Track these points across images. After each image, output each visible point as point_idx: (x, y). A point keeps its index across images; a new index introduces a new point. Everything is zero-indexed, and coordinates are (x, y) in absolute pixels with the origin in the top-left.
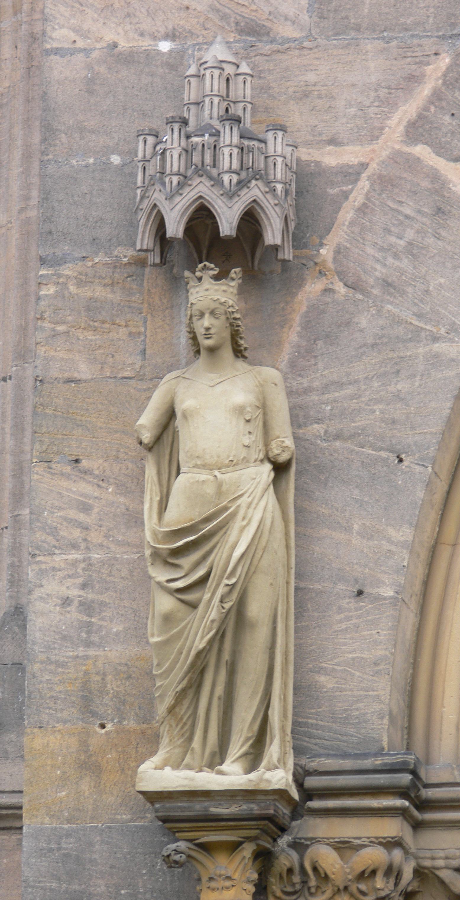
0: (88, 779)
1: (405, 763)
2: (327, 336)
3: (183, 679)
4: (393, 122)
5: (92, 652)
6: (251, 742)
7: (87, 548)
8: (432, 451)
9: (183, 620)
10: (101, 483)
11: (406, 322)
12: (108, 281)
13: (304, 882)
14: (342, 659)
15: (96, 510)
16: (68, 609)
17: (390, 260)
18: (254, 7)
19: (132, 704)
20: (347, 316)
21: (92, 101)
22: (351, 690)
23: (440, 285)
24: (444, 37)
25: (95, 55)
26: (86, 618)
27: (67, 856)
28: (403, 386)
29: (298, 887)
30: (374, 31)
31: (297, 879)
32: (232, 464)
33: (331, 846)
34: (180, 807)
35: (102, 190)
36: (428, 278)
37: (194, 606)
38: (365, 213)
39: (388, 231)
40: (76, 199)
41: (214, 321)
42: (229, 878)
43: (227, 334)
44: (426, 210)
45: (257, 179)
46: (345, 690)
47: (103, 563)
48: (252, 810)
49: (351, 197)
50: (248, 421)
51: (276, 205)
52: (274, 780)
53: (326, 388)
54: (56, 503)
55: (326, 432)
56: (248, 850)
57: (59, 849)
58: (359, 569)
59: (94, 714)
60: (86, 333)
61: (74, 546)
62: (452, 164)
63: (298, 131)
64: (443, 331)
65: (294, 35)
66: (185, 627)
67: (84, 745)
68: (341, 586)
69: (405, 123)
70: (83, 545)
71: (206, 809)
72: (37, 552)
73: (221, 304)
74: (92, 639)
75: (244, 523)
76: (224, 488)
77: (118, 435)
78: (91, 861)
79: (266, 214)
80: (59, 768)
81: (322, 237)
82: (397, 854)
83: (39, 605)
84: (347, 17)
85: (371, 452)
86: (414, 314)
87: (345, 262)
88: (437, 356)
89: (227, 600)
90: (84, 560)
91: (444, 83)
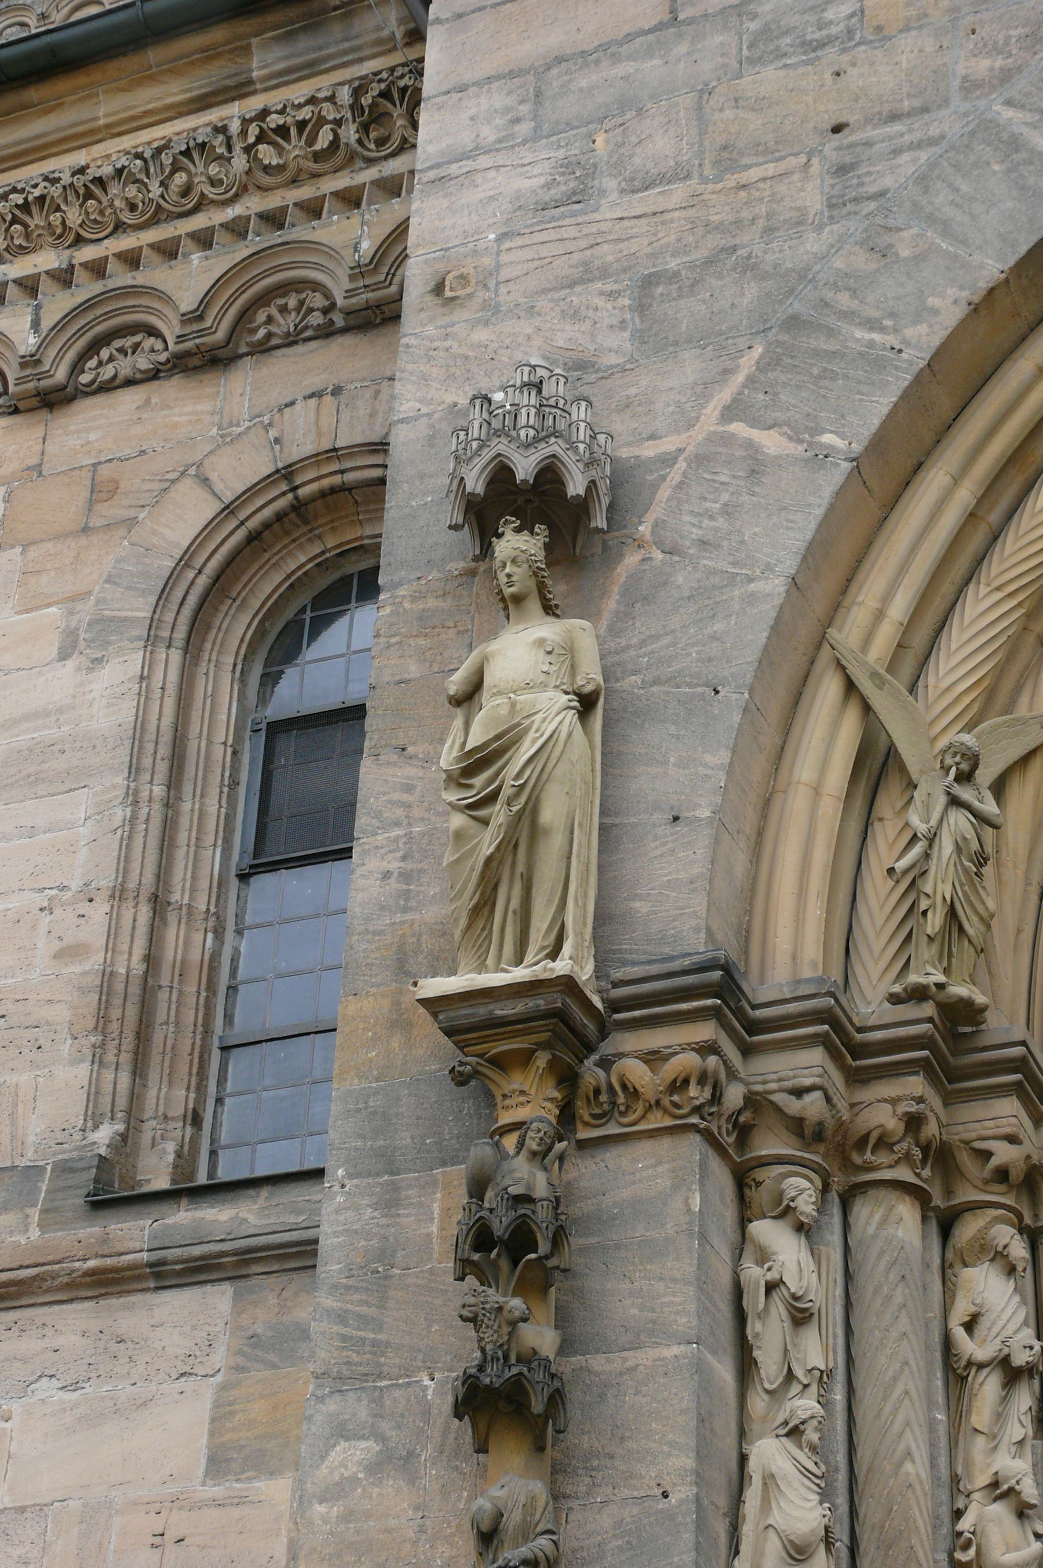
0: (399, 1036)
1: (715, 959)
2: (645, 598)
3: (474, 894)
4: (708, 411)
5: (409, 917)
6: (547, 951)
7: (409, 823)
8: (749, 678)
9: (473, 837)
10: (425, 764)
11: (722, 572)
12: (440, 592)
13: (614, 1104)
14: (658, 883)
15: (418, 789)
16: (388, 881)
17: (706, 522)
18: (581, 349)
19: (446, 959)
20: (664, 578)
21: (433, 452)
22: (666, 911)
23: (755, 534)
24: (758, 333)
25: (436, 416)
26: (404, 887)
27: (374, 1113)
28: (719, 627)
29: (606, 1107)
30: (691, 342)
31: (604, 1098)
32: (528, 686)
33: (640, 1059)
34: (464, 1015)
35: (439, 520)
36: (743, 530)
37: (485, 822)
38: (681, 489)
39: (704, 499)
40: (414, 532)
41: (516, 569)
42: (522, 1092)
43: (532, 583)
44: (740, 474)
45: (556, 437)
46: (660, 912)
47: (423, 834)
48: (538, 1006)
49: (669, 479)
50: (549, 653)
51: (578, 461)
52: (558, 968)
53: (643, 643)
54: (382, 789)
55: (643, 680)
56: (542, 1059)
57: (366, 1108)
58: (675, 797)
59: (408, 974)
60: (417, 640)
61: (397, 824)
62: (766, 432)
63: (620, 435)
64: (758, 572)
65: (617, 362)
66: (478, 844)
67: (397, 1003)
68: (657, 816)
69: (720, 408)
70: (405, 822)
71: (491, 1013)
72: (361, 836)
73: (522, 551)
74: (409, 905)
75: (537, 735)
76: (518, 707)
77: (442, 720)
78: (397, 1115)
79: (567, 468)
80: (370, 1030)
81: (640, 517)
82: (712, 1060)
83: (361, 882)
84: (666, 338)
85: (687, 690)
86: (730, 563)
87: (662, 532)
88: (752, 594)
89: (514, 803)
90: (406, 835)
91: (758, 369)
